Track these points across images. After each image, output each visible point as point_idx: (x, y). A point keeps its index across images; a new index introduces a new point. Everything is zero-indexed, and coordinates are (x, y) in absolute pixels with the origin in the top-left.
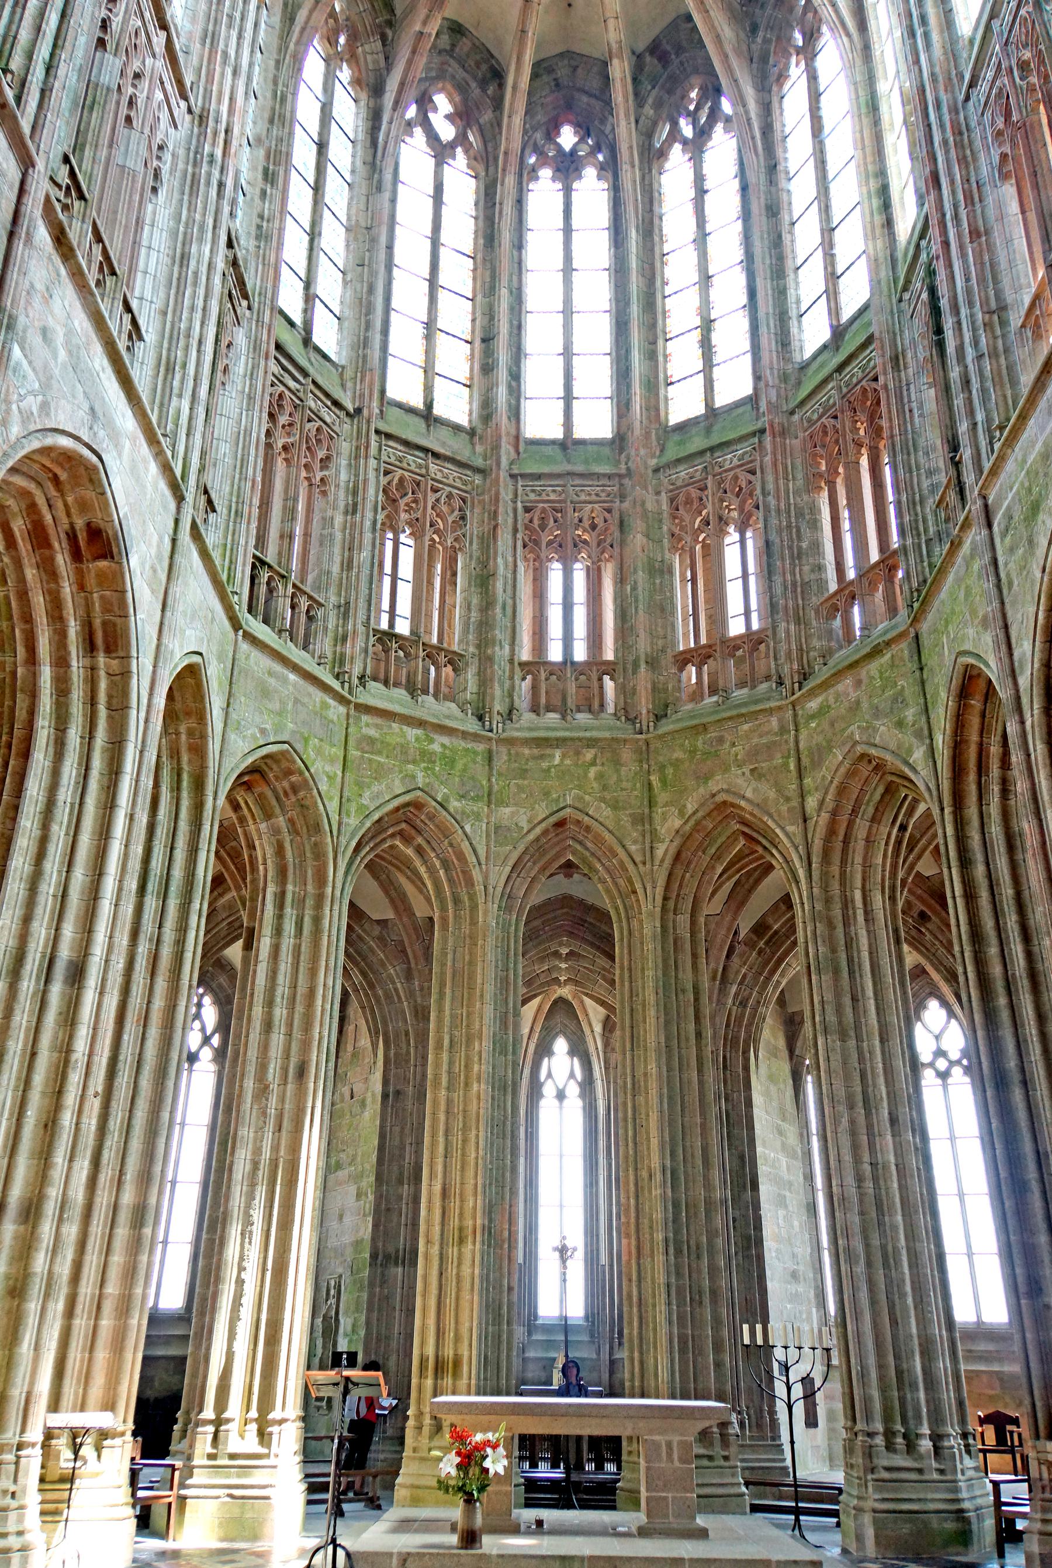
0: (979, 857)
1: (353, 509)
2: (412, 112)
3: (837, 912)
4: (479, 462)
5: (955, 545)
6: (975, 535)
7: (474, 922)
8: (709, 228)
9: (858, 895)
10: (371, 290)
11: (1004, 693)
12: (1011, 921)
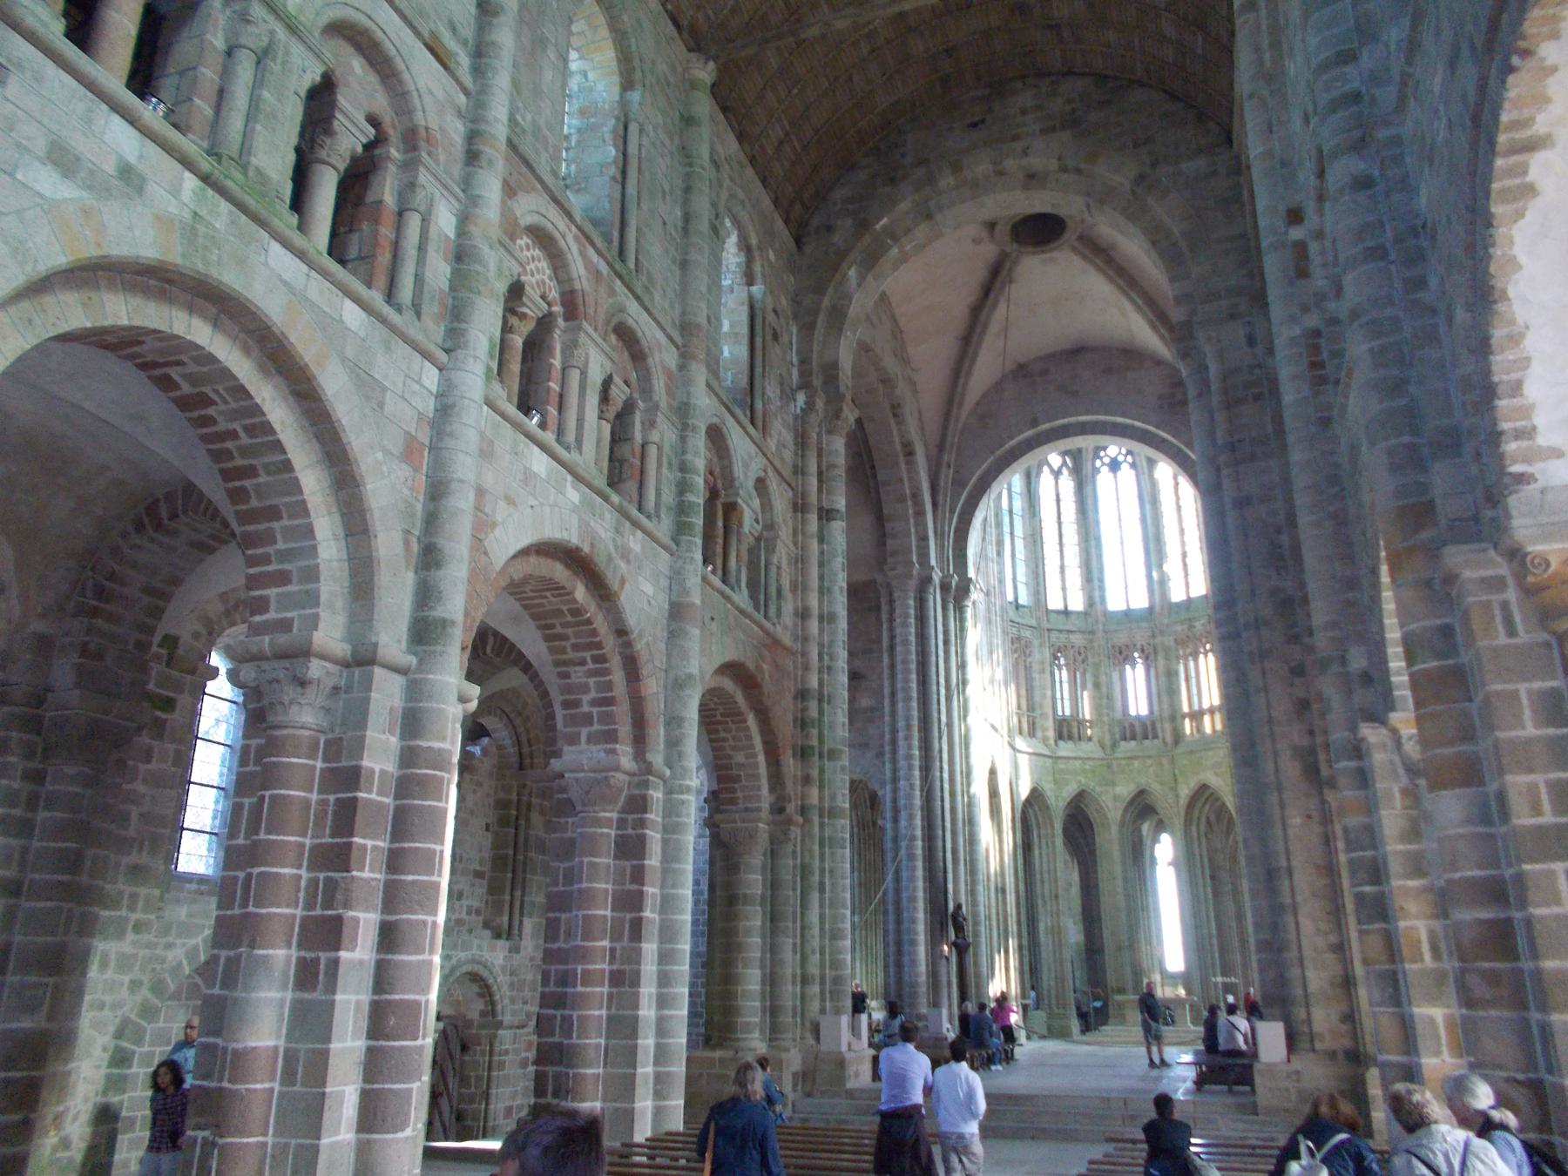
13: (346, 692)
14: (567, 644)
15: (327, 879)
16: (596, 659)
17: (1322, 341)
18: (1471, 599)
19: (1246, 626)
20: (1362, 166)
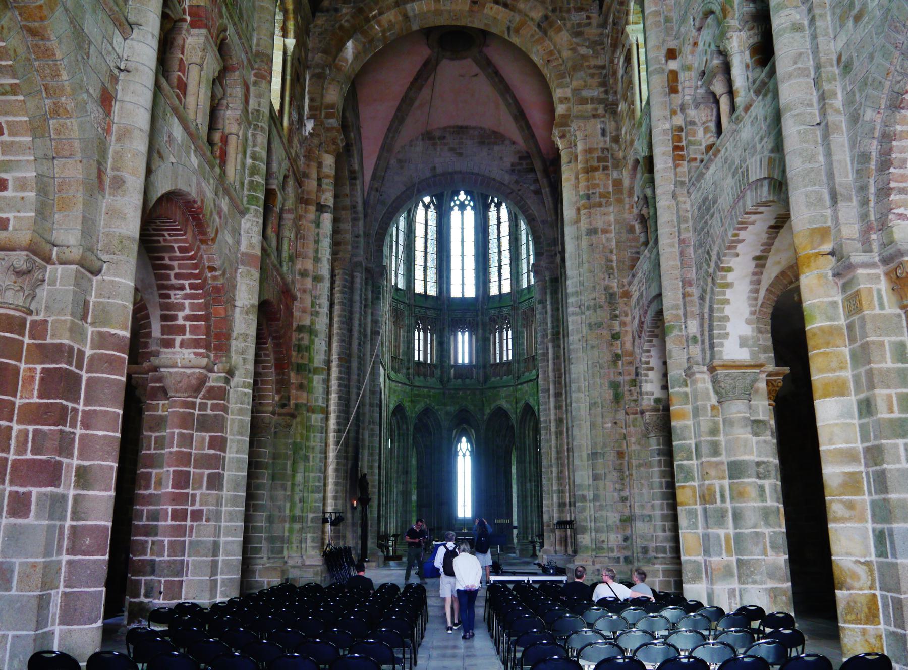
1: (409, 332)
8: (502, 235)
13: (49, 285)
14: (172, 273)
15: (35, 431)
16: (192, 286)
17: (683, 134)
18: (861, 286)
19: (588, 308)
20: (798, 17)
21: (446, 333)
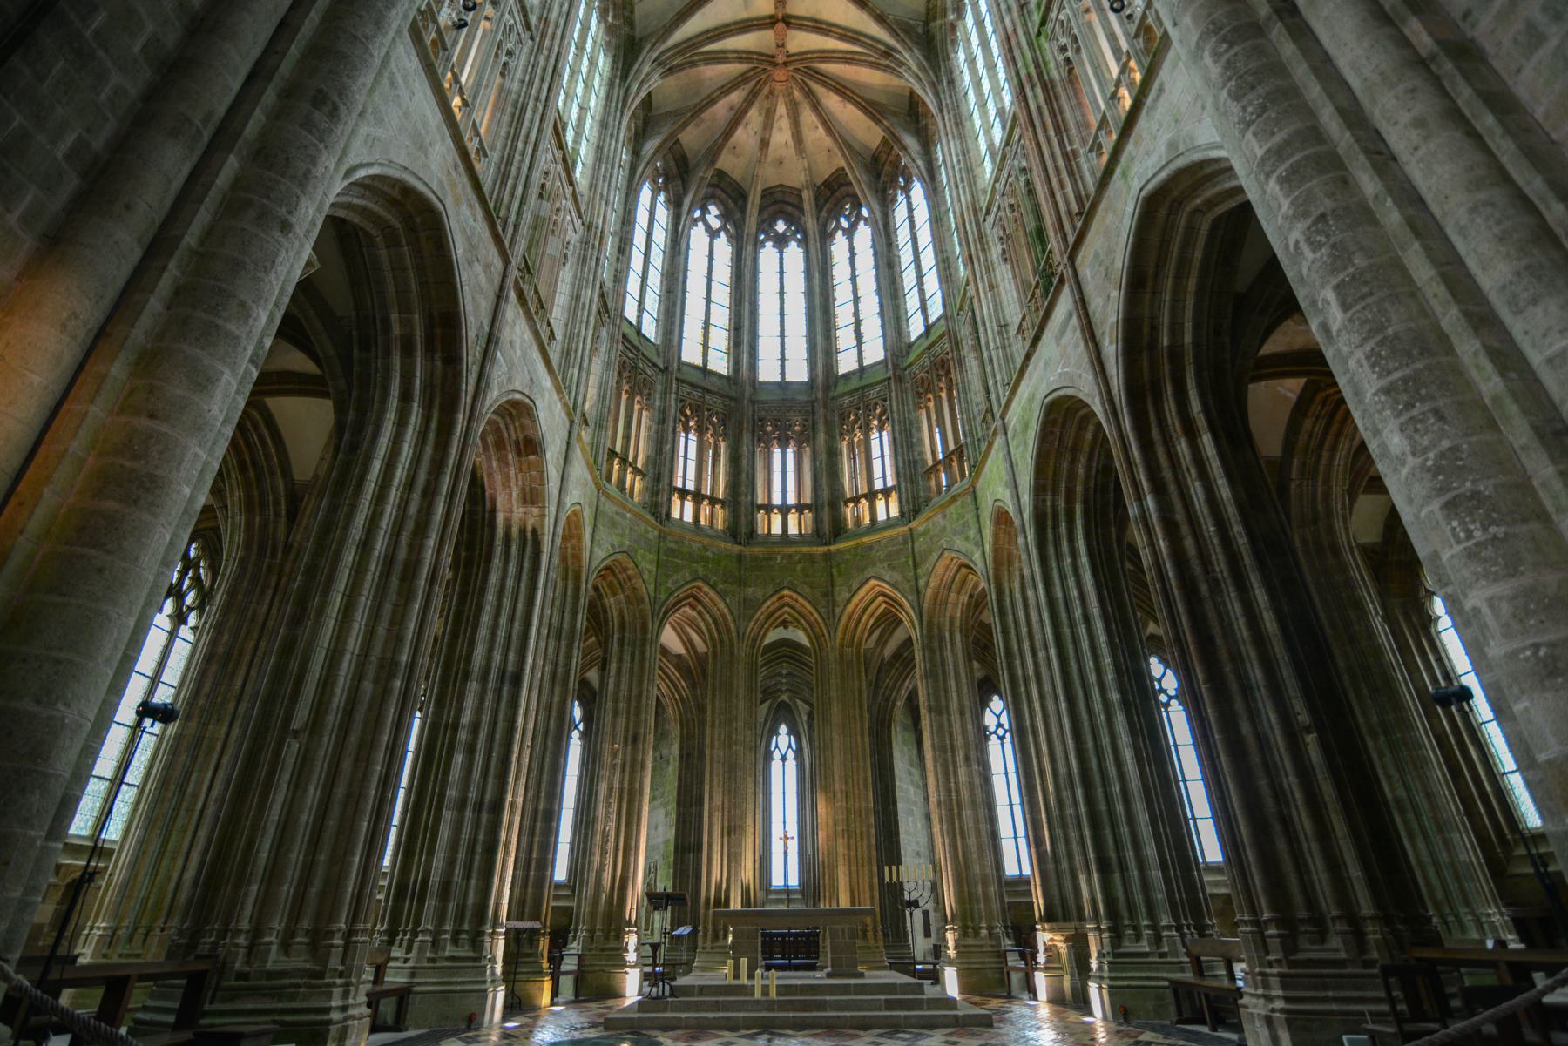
0: (1010, 611)
1: (662, 421)
2: (697, 214)
3: (936, 644)
4: (733, 394)
5: (990, 444)
6: (999, 441)
7: (732, 654)
9: (947, 634)
10: (674, 305)
11: (1017, 523)
12: (1026, 645)
21: (746, 437)
